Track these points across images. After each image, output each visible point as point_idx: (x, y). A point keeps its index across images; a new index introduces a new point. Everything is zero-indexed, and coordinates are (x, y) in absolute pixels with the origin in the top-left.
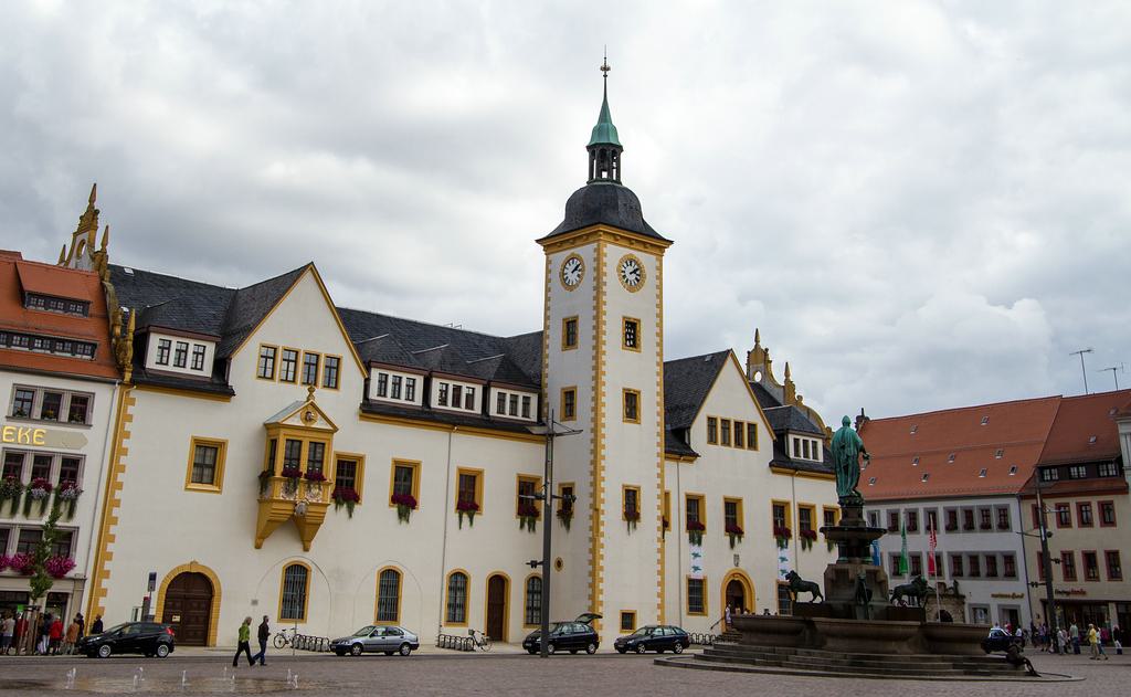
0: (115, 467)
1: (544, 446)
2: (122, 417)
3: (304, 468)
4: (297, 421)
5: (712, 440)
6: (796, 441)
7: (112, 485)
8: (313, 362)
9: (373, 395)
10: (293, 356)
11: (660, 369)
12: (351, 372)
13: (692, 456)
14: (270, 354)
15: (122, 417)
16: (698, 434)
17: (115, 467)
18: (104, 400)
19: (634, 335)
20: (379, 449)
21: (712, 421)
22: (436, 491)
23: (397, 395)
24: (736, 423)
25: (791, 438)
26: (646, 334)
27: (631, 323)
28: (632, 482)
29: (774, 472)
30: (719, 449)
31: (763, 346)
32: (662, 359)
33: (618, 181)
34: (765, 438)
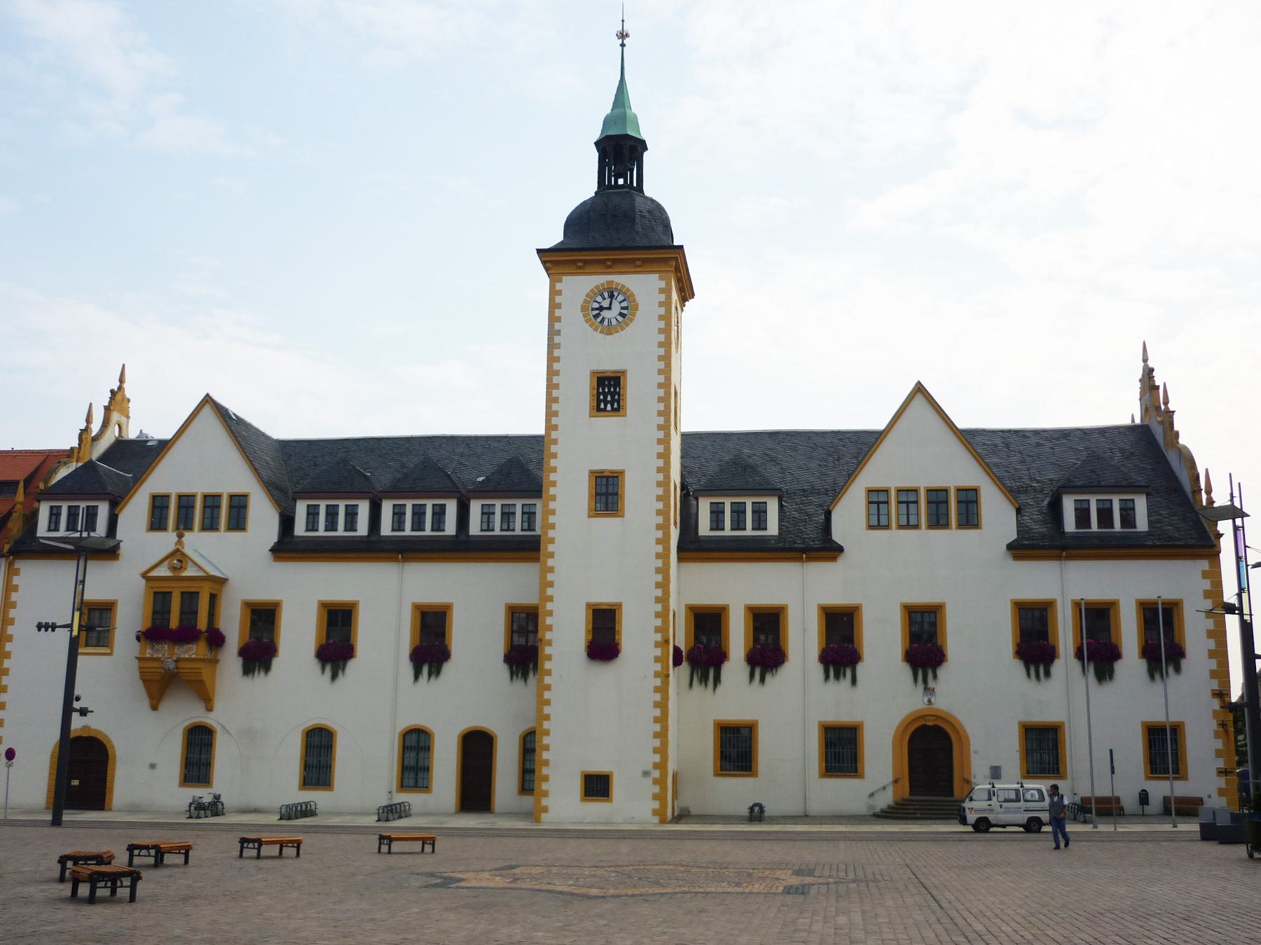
1: (75, 562)
4: (163, 571)
8: (938, 498)
9: (300, 529)
10: (908, 496)
13: (828, 549)
14: (877, 498)
16: (848, 517)
19: (619, 394)
20: (302, 592)
21: (877, 498)
22: (383, 636)
23: (332, 526)
25: (1069, 505)
26: (638, 392)
27: (609, 379)
28: (604, 597)
33: (640, 187)
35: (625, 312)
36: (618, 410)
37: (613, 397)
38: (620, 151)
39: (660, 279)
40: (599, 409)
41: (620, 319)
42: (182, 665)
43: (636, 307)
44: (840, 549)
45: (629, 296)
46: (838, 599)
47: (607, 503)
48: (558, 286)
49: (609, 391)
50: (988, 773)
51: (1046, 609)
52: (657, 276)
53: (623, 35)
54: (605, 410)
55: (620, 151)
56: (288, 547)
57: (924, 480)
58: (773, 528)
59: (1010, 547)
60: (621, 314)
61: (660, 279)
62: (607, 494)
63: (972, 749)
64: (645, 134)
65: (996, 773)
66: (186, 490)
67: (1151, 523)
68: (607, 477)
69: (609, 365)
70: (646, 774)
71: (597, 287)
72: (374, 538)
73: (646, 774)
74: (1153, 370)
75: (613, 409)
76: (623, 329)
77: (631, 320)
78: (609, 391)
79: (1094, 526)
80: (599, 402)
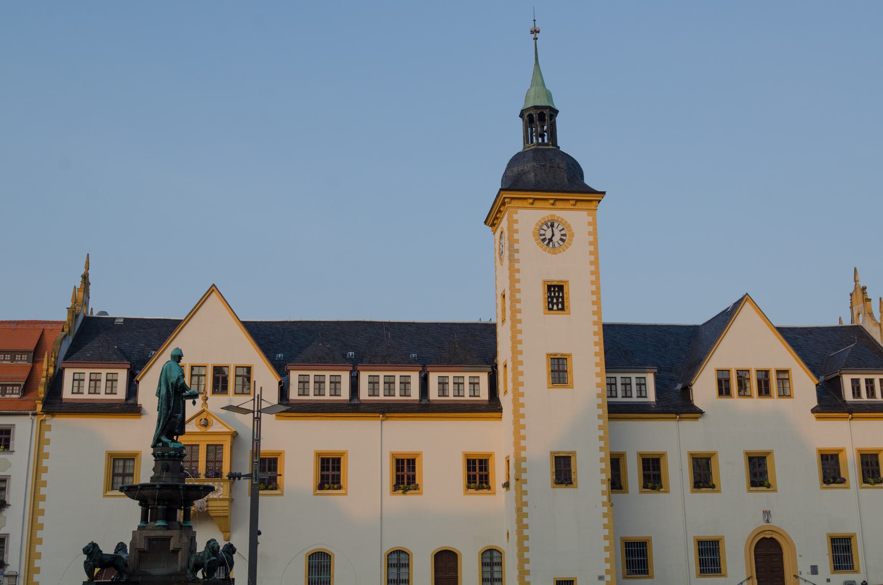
0: (37, 483)
2: (41, 442)
3: (226, 470)
5: (724, 389)
6: (855, 383)
7: (36, 497)
9: (294, 394)
11: (599, 329)
12: (266, 379)
13: (696, 412)
15: (41, 442)
16: (703, 389)
17: (37, 483)
18: (23, 429)
19: (563, 297)
24: (738, 371)
25: (847, 380)
26: (574, 296)
27: (554, 286)
29: (818, 418)
30: (735, 402)
31: (862, 284)
32: (600, 318)
34: (805, 385)
35: (564, 238)
36: (563, 309)
37: (557, 300)
38: (540, 119)
39: (589, 215)
40: (549, 309)
41: (561, 243)
42: (211, 504)
43: (572, 235)
44: (701, 412)
45: (566, 226)
46: (701, 448)
47: (559, 378)
48: (515, 217)
49: (556, 296)
50: (809, 570)
51: (710, 459)
52: (585, 213)
53: (535, 31)
54: (551, 309)
55: (540, 119)
56: (288, 408)
57: (753, 363)
58: (651, 397)
59: (814, 411)
60: (561, 239)
61: (589, 215)
62: (559, 371)
63: (798, 554)
64: (557, 106)
65: (814, 570)
66: (763, 366)
67: (657, 396)
68: (558, 359)
69: (555, 278)
70: (601, 578)
71: (543, 218)
72: (356, 402)
73: (601, 578)
74: (864, 289)
75: (558, 309)
76: (564, 250)
77: (570, 244)
78: (556, 296)
79: (864, 397)
80: (549, 303)
